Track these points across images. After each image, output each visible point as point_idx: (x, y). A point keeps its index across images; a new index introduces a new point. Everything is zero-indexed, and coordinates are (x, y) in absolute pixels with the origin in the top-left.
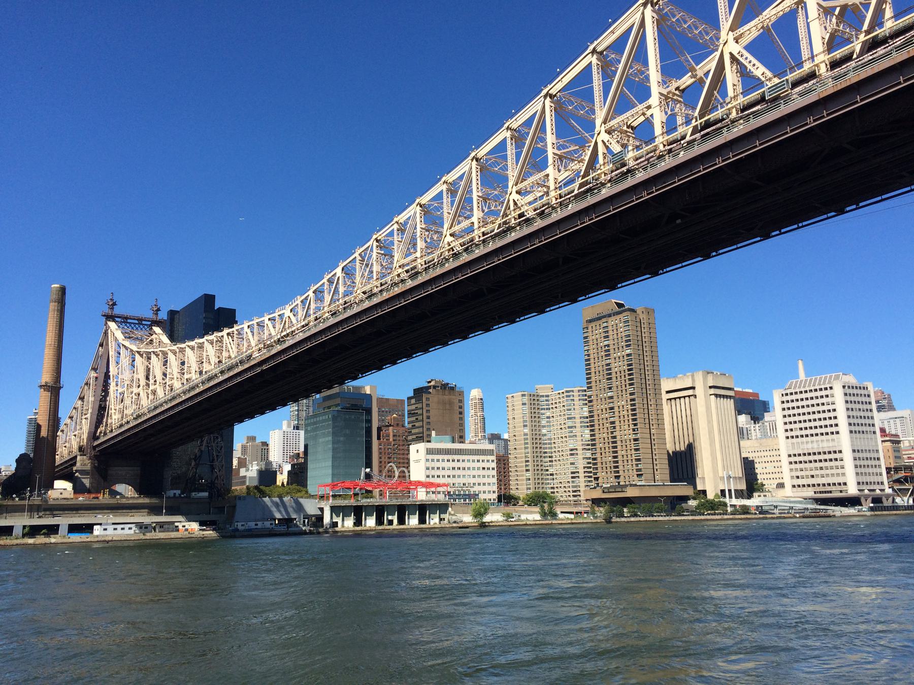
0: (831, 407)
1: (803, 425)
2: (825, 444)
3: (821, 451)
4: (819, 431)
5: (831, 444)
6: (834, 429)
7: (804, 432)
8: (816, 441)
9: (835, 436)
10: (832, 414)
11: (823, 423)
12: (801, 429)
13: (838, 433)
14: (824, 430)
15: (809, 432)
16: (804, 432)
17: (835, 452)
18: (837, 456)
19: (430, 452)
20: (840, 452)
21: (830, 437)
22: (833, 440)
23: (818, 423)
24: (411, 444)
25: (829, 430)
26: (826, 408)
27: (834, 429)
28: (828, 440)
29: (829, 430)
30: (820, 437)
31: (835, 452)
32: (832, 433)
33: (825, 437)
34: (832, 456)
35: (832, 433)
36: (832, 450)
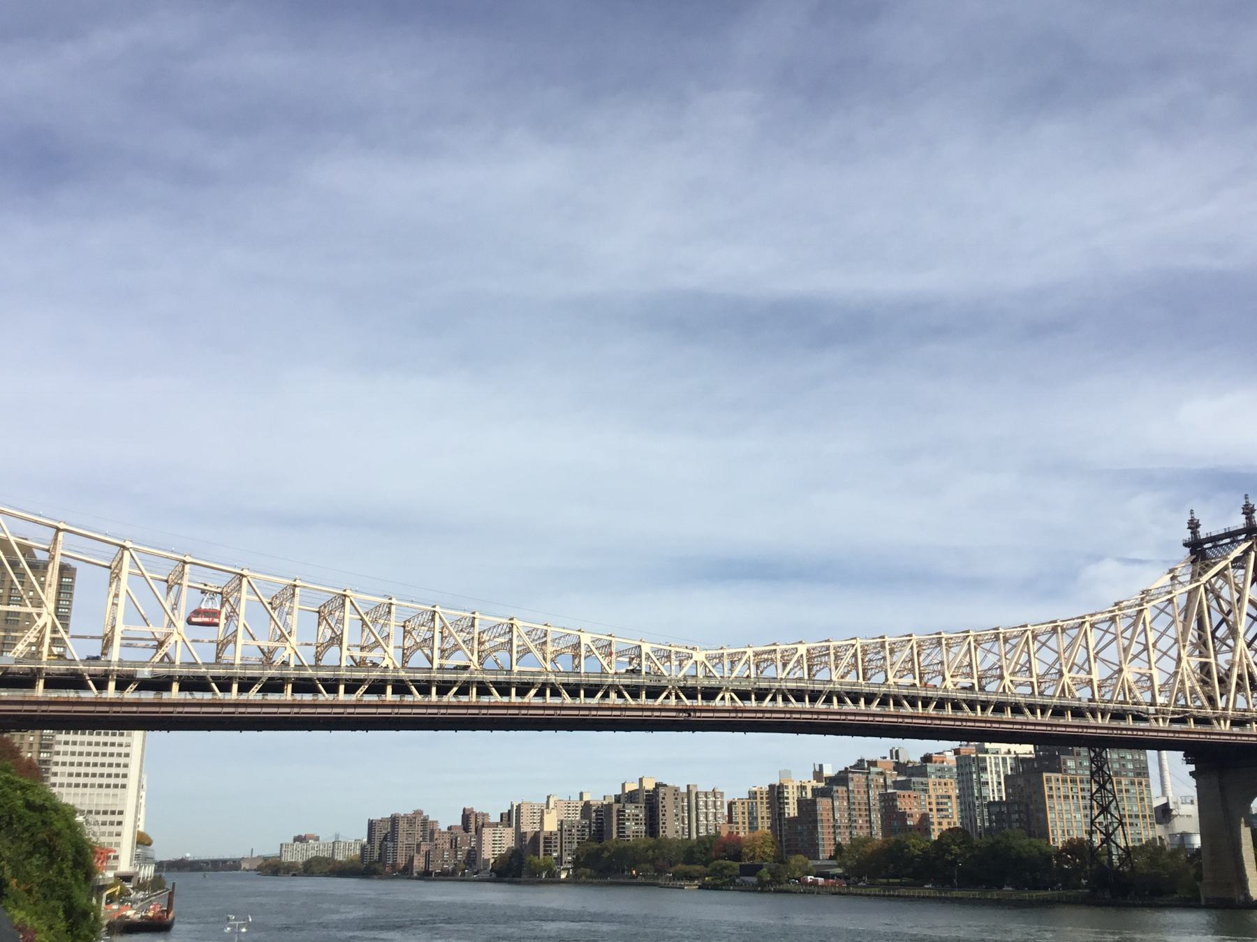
0: (123, 750)
1: (75, 770)
2: (103, 801)
3: (94, 809)
4: (97, 781)
5: (111, 801)
6: (120, 781)
7: (74, 780)
8: (90, 794)
9: (119, 791)
10: (122, 760)
11: (106, 770)
12: (70, 775)
13: (124, 786)
14: (105, 781)
15: (81, 780)
16: (74, 780)
17: (113, 813)
18: (116, 818)
20: (121, 813)
21: (111, 791)
22: (115, 795)
23: (98, 770)
25: (112, 781)
26: (115, 750)
27: (120, 781)
28: (107, 795)
29: (112, 781)
30: (97, 790)
31: (113, 813)
32: (116, 786)
33: (104, 790)
34: (109, 818)
35: (116, 786)
36: (109, 809)
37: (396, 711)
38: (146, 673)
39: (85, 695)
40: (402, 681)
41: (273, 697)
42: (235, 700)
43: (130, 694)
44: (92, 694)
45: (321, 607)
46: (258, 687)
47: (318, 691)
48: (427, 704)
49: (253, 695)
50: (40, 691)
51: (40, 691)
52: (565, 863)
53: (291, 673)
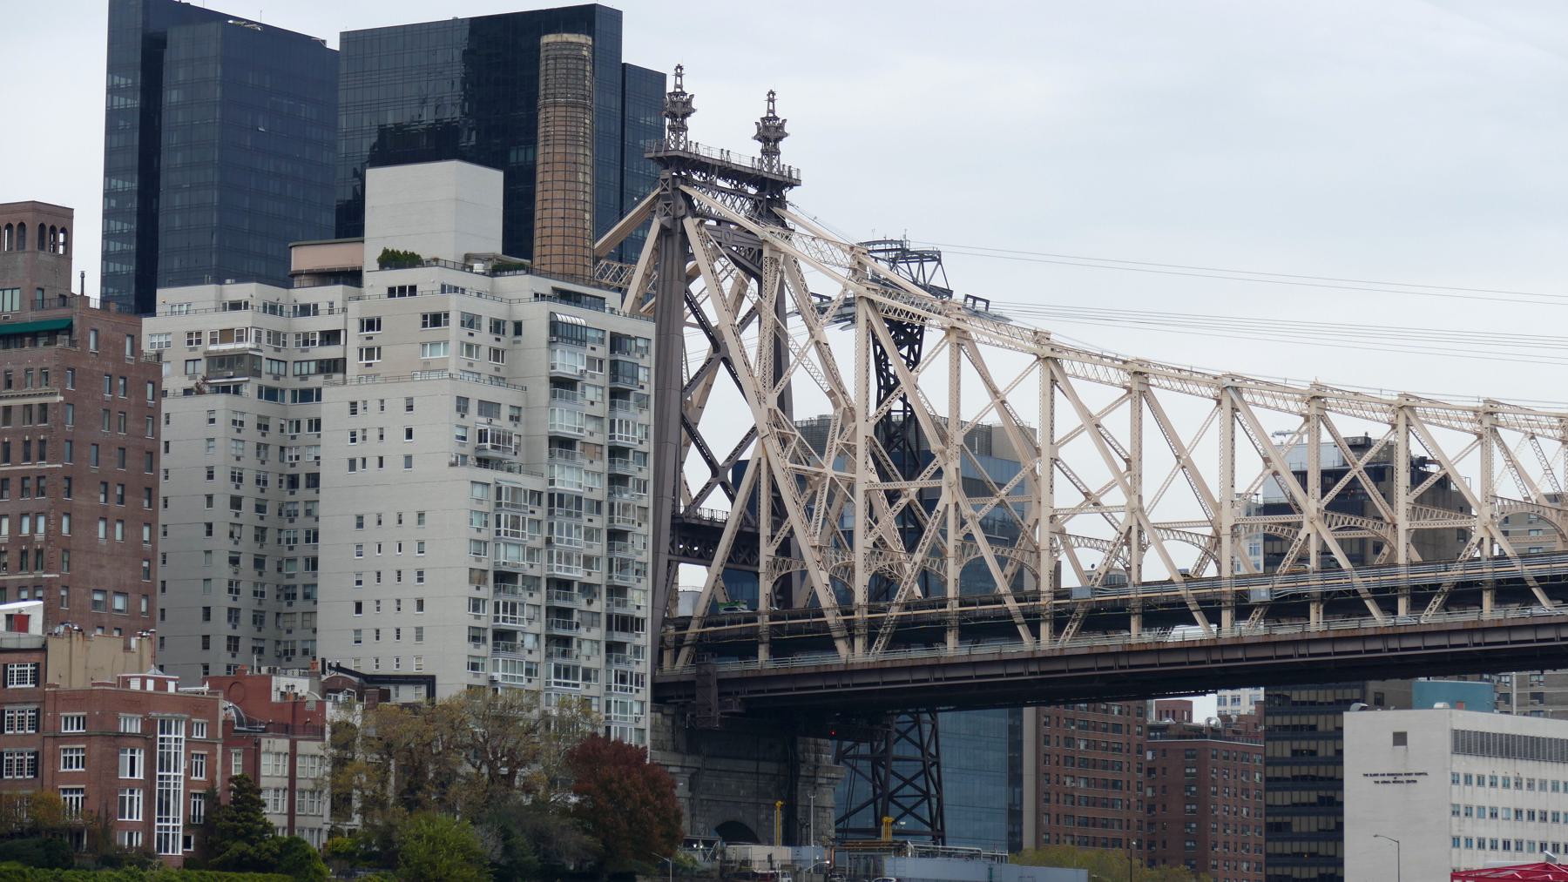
19: (1465, 743)
24: (1346, 704)
37: (1303, 650)
38: (1263, 594)
39: (1009, 649)
40: (1521, 580)
41: (1286, 630)
42: (1033, 652)
43: (1431, 616)
44: (1379, 618)
45: (1438, 463)
46: (1437, 601)
47: (1532, 600)
48: (1510, 624)
49: (1431, 616)
50: (952, 647)
51: (952, 647)
52: (772, 869)
53: (1488, 573)
